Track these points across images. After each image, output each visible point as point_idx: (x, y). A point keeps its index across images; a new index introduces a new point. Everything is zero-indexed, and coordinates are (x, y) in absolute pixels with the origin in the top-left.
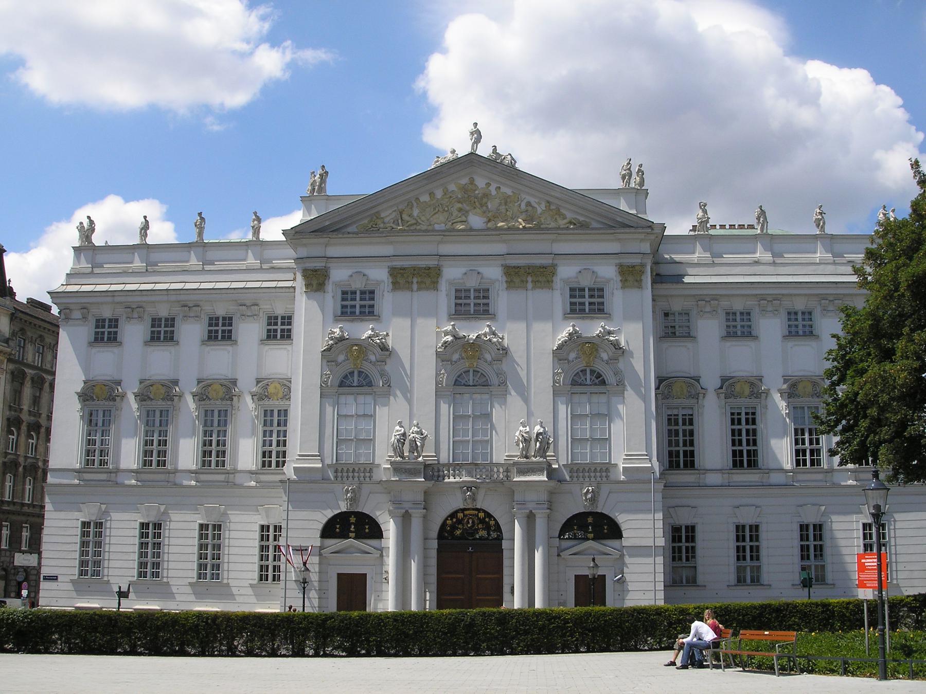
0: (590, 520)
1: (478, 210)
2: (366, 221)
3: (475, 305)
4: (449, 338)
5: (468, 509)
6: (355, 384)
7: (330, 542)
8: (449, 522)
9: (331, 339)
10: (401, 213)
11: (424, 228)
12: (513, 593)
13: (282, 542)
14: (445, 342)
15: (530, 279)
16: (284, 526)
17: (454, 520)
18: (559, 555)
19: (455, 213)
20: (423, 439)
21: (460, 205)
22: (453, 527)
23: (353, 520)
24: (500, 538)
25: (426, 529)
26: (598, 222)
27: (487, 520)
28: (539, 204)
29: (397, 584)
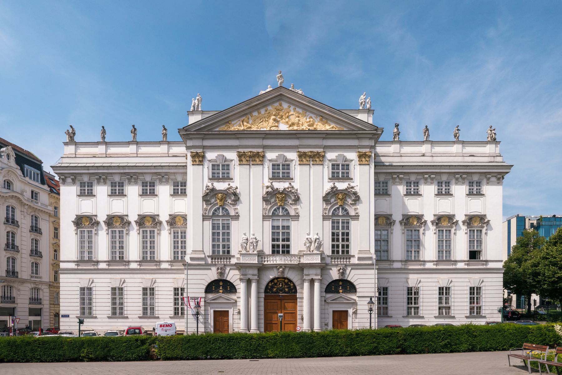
0: (341, 283)
1: (284, 120)
2: (224, 126)
3: (282, 173)
4: (270, 189)
5: (280, 278)
6: (221, 214)
7: (210, 296)
8: (270, 284)
9: (208, 189)
10: (243, 122)
11: (255, 129)
12: (302, 319)
13: (185, 295)
14: (267, 192)
15: (311, 159)
16: (185, 287)
18: (325, 301)
19: (271, 121)
20: (257, 242)
21: (274, 117)
22: (272, 287)
23: (221, 284)
24: (296, 292)
25: (258, 288)
26: (348, 128)
28: (316, 118)
29: (244, 315)
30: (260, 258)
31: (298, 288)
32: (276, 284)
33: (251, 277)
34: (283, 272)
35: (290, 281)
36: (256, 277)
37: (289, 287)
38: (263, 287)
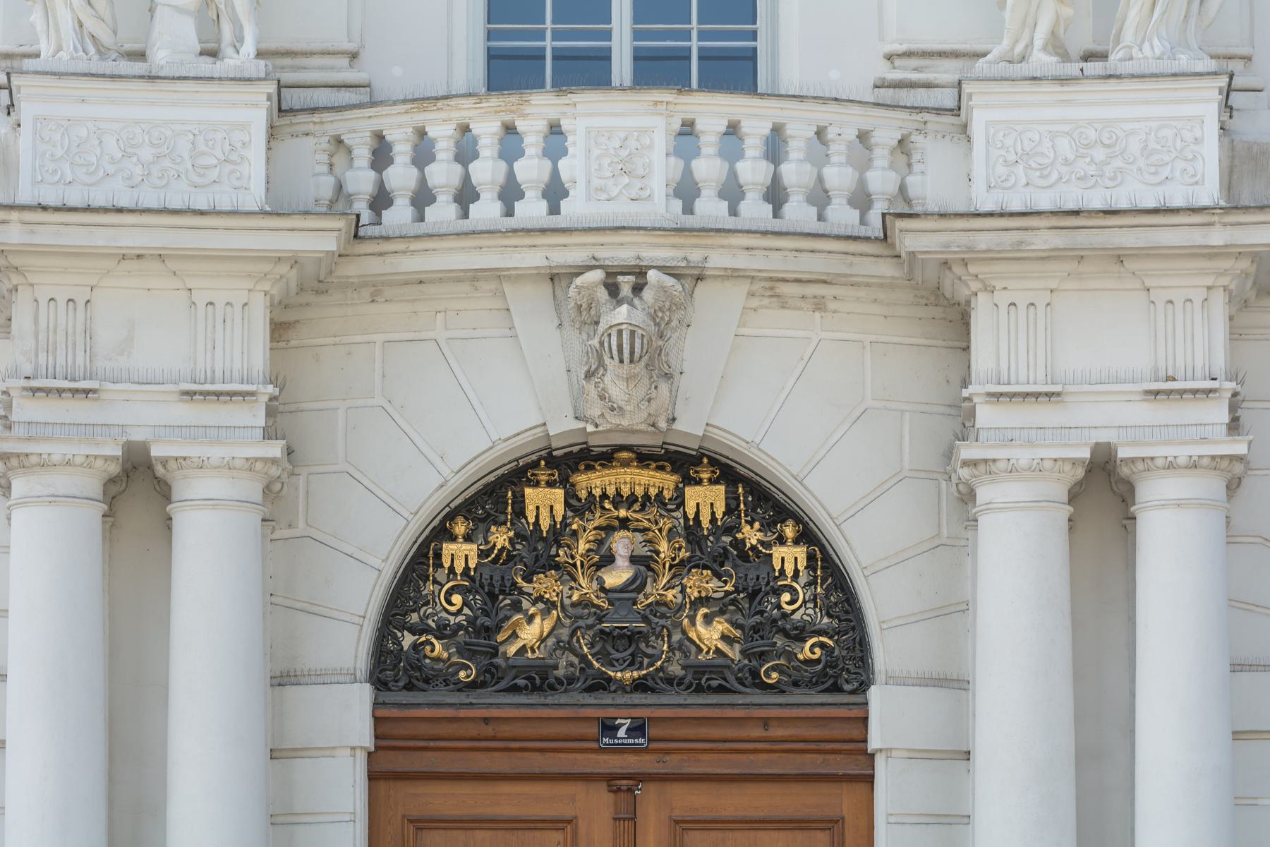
17: (501, 538)
22: (494, 592)
25: (281, 604)
27: (751, 535)
30: (307, 153)
31: (882, 601)
32: (541, 550)
33: (150, 419)
34: (651, 357)
35: (760, 499)
36: (242, 435)
37: (753, 596)
38: (361, 593)
